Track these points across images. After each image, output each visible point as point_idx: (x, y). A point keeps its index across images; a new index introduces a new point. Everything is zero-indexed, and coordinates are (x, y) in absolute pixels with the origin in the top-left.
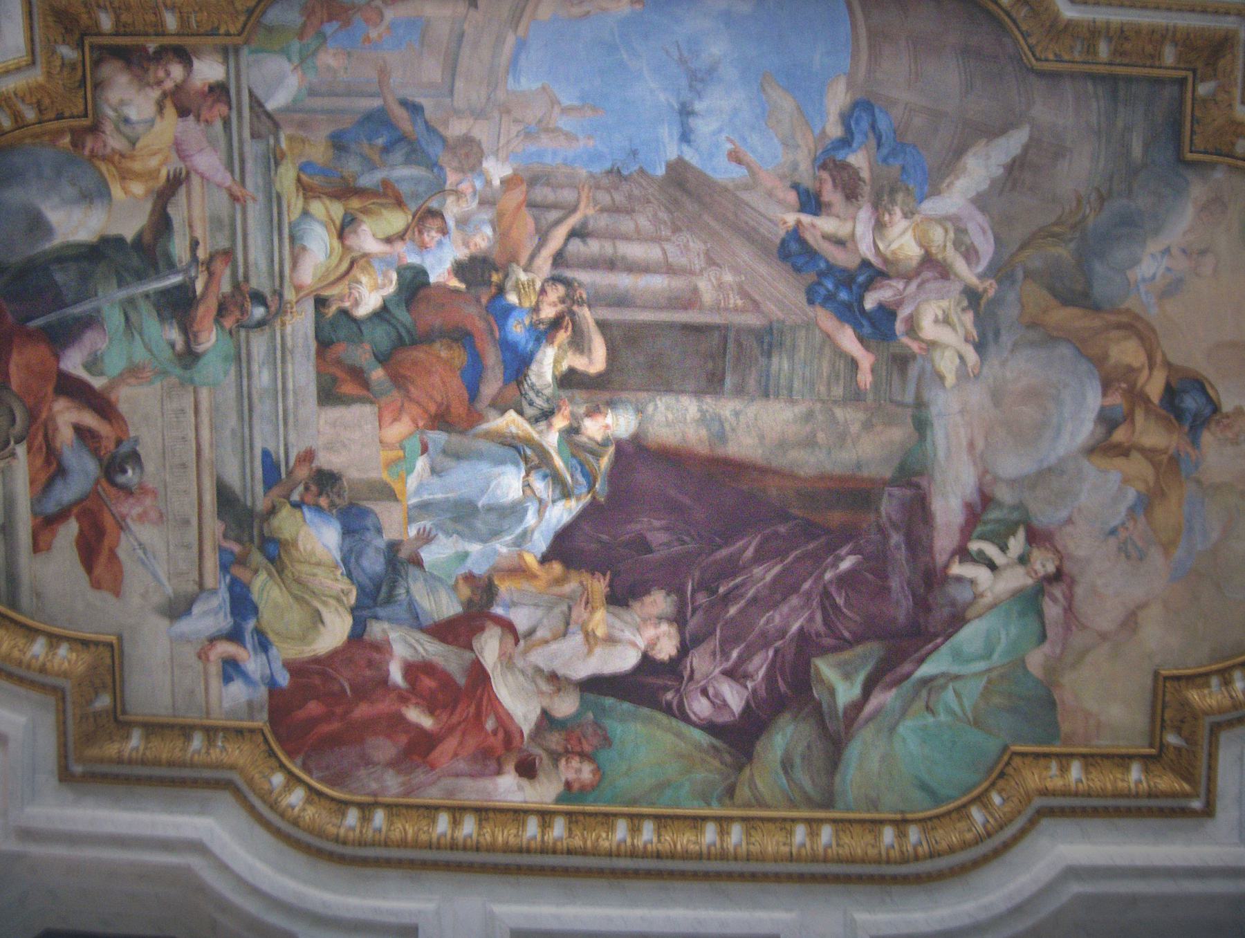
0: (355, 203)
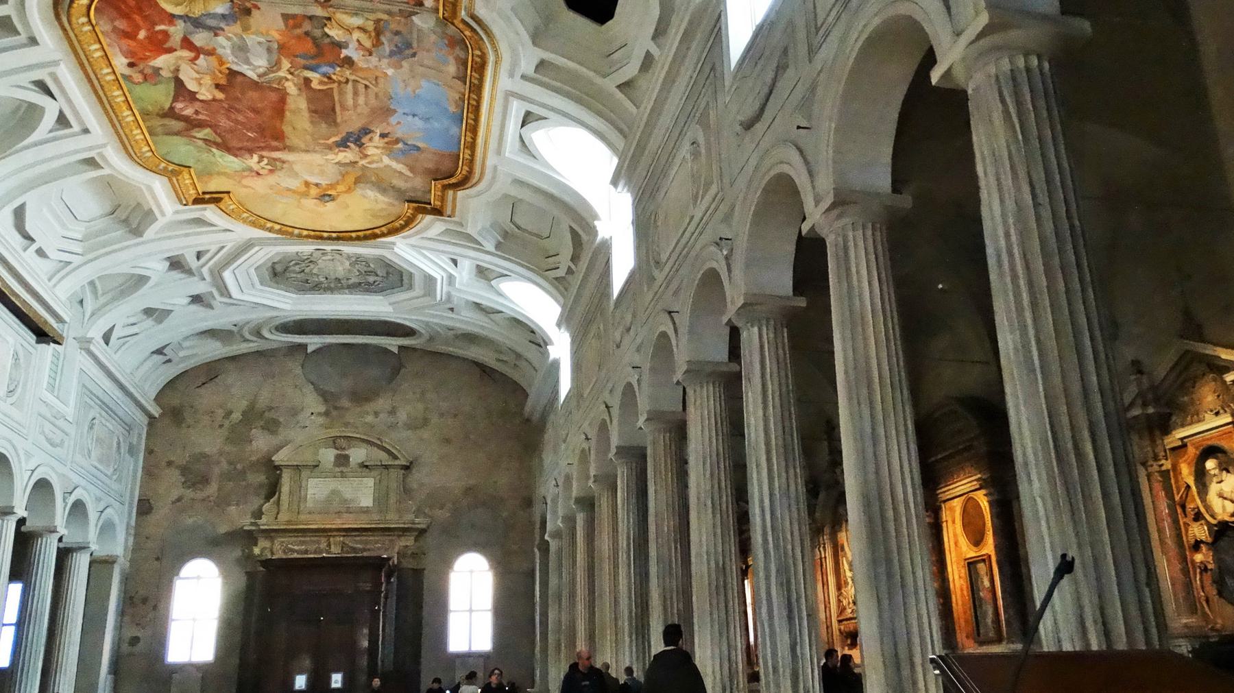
0: (373, 34)
